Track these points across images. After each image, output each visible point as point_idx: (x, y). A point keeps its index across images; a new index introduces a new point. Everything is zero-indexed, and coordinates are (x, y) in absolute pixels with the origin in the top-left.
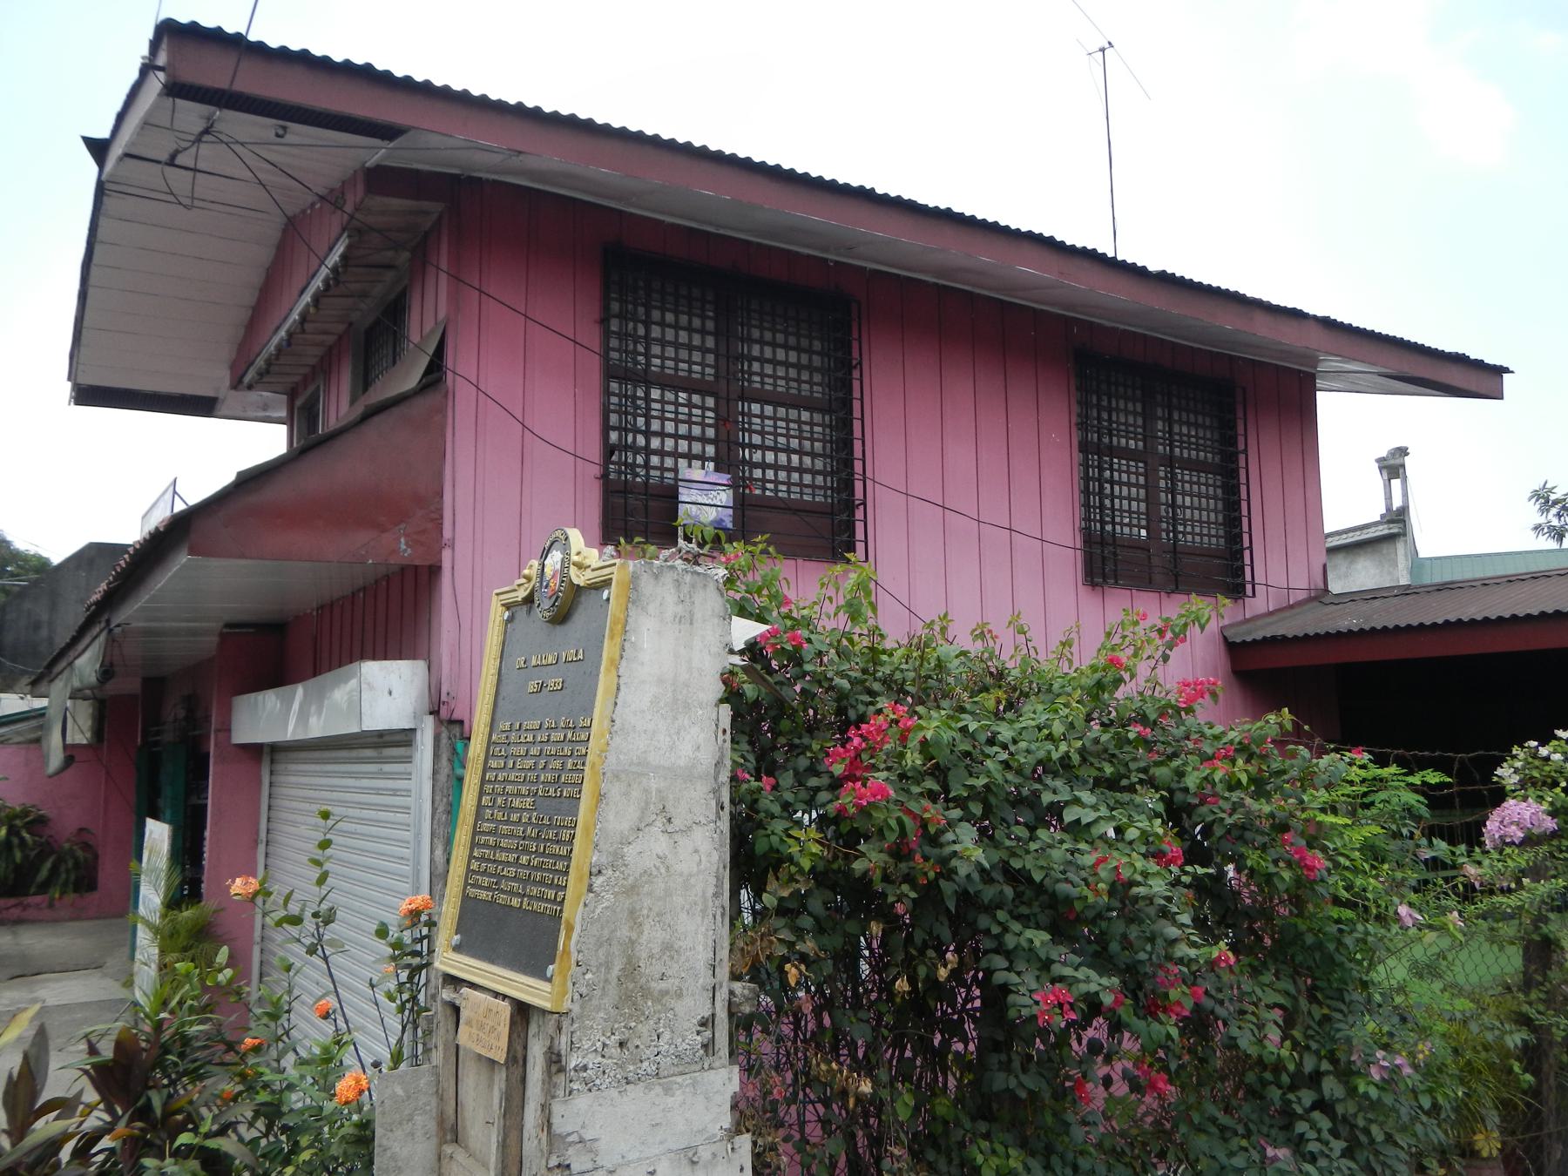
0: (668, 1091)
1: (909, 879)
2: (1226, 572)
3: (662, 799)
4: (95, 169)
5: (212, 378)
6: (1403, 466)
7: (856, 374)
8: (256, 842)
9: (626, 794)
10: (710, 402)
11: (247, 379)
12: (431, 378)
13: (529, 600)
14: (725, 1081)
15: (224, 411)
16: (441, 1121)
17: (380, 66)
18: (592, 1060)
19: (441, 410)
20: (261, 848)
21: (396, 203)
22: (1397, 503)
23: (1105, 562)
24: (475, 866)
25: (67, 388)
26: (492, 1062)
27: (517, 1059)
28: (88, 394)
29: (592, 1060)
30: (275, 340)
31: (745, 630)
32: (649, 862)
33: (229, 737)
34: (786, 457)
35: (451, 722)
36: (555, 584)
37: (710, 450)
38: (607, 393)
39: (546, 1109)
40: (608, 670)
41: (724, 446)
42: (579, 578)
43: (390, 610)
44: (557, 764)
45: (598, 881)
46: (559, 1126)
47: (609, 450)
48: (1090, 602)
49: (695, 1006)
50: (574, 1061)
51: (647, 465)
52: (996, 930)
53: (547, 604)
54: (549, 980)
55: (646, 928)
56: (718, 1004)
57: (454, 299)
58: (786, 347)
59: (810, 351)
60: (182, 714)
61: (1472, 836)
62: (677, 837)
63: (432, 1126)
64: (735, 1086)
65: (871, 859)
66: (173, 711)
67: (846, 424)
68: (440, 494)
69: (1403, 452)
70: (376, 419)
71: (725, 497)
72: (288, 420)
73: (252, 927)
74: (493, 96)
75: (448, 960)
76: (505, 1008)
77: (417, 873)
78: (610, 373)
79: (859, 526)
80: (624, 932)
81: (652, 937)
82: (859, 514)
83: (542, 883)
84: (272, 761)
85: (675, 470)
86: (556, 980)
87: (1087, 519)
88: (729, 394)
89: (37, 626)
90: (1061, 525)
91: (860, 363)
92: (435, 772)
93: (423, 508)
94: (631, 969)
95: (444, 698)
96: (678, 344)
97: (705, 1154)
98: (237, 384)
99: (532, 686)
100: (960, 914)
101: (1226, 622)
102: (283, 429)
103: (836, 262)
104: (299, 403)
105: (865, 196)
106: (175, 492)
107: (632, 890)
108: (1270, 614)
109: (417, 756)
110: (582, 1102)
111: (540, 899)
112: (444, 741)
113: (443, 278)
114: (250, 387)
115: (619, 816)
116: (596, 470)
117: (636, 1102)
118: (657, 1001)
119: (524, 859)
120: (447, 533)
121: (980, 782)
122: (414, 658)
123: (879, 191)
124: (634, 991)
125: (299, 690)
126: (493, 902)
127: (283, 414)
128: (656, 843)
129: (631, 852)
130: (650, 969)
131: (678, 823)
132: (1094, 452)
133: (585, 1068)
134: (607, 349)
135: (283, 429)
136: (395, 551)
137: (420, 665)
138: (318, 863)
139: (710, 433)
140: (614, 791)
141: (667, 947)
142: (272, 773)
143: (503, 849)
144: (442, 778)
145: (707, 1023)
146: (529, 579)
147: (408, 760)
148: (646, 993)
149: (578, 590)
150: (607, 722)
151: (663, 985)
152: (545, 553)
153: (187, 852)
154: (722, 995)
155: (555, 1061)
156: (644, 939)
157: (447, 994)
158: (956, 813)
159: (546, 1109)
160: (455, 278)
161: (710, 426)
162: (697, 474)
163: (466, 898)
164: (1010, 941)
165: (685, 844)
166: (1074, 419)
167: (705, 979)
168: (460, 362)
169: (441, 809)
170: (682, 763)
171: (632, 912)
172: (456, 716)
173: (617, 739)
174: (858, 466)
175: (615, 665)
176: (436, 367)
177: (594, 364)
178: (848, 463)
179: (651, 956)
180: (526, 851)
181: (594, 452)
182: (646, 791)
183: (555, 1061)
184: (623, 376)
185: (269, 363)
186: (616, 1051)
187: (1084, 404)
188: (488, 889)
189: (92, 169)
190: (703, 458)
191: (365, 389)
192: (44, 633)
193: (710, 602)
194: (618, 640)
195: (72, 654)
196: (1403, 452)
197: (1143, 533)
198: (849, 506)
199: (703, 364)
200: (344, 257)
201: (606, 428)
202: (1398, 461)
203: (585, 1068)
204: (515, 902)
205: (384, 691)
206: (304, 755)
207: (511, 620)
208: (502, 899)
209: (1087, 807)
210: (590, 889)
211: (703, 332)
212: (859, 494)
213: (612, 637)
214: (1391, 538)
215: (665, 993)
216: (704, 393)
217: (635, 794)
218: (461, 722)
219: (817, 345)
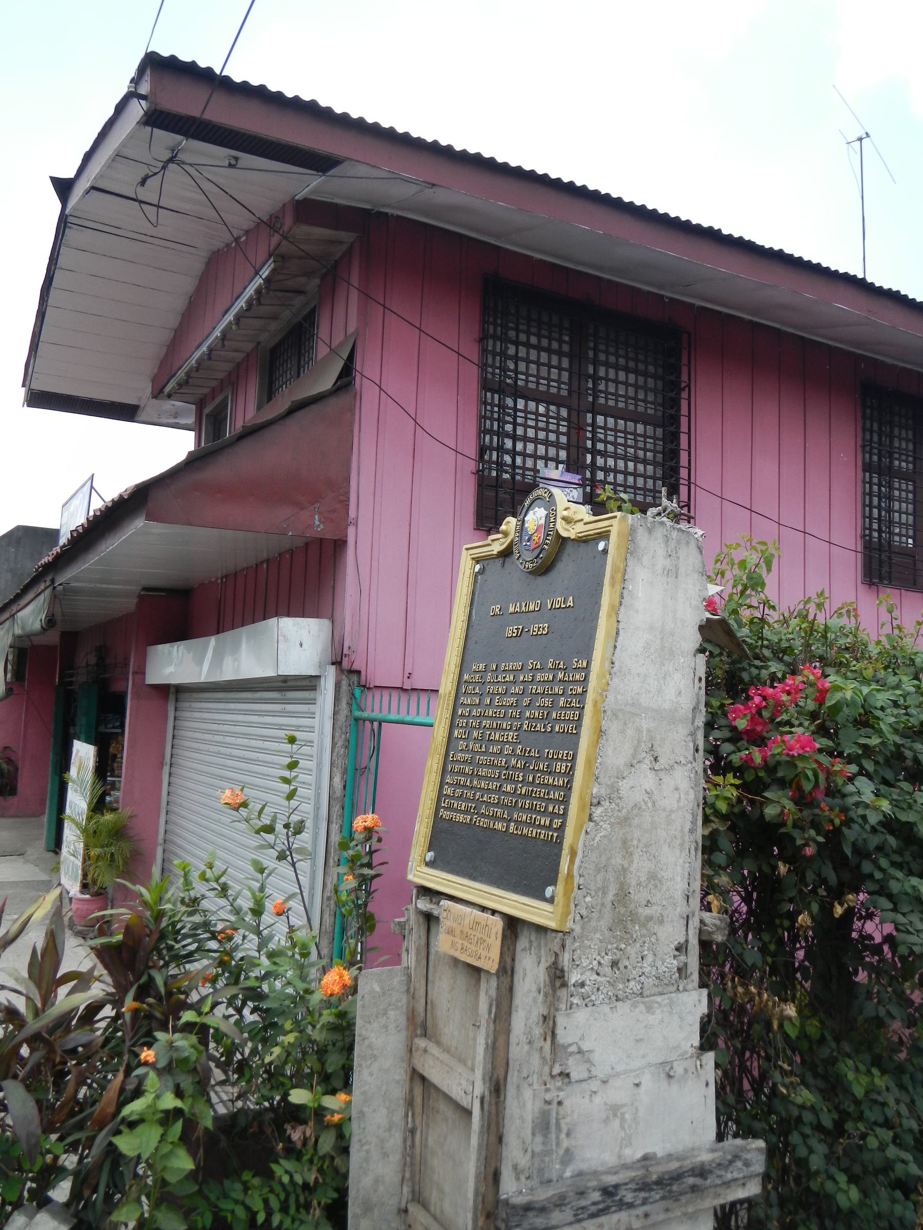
0: (649, 1009)
1: (815, 824)
3: (652, 738)
4: (59, 206)
5: (134, 389)
7: (684, 395)
8: (162, 765)
9: (622, 732)
10: (564, 413)
11: (167, 389)
12: (345, 380)
13: (506, 553)
14: (695, 1003)
15: (143, 415)
16: (411, 1017)
17: (323, 103)
18: (589, 977)
19: (352, 410)
20: (166, 769)
21: (319, 232)
24: (448, 791)
25: (22, 393)
26: (476, 971)
27: (507, 970)
28: (39, 398)
29: (589, 977)
30: (197, 355)
33: (144, 678)
35: (351, 672)
36: (538, 538)
37: (563, 454)
39: (549, 1022)
40: (609, 616)
41: (573, 450)
43: (302, 575)
44: (547, 702)
45: (598, 811)
46: (563, 1037)
47: (482, 450)
49: (672, 932)
50: (574, 977)
52: (878, 875)
53: (528, 556)
54: (551, 901)
55: (636, 857)
56: (691, 932)
57: (363, 314)
58: (627, 370)
59: (645, 374)
60: (93, 660)
62: (662, 775)
63: (403, 1020)
64: (703, 1009)
65: (778, 805)
66: (86, 658)
70: (299, 414)
72: (196, 427)
73: (157, 832)
74: (415, 134)
75: (420, 873)
76: (497, 924)
77: (318, 796)
78: (486, 385)
80: (618, 860)
81: (640, 866)
83: (532, 809)
84: (177, 700)
85: (536, 471)
86: (559, 899)
88: (578, 406)
90: (846, 533)
91: (689, 386)
92: (335, 713)
93: (335, 492)
94: (623, 895)
95: (346, 651)
96: (540, 366)
97: (679, 1069)
98: (158, 393)
99: (510, 631)
102: (192, 434)
103: (671, 299)
104: (207, 411)
105: (712, 236)
106: (92, 487)
107: (625, 821)
109: (320, 701)
110: (581, 1016)
111: (532, 824)
112: (344, 687)
113: (354, 295)
114: (169, 396)
115: (616, 753)
116: (472, 466)
117: (623, 1018)
118: (643, 925)
119: (509, 788)
122: (317, 616)
123: (725, 232)
124: (626, 919)
125: (213, 641)
126: (471, 825)
127: (191, 420)
128: (644, 779)
129: (624, 785)
130: (638, 896)
131: (662, 760)
133: (583, 985)
135: (192, 434)
136: (311, 526)
137: (325, 623)
138: (287, 781)
139: (563, 439)
140: (612, 727)
142: (176, 709)
143: (480, 777)
144: (342, 717)
145: (681, 948)
146: (506, 534)
147: (313, 702)
148: (634, 917)
149: (562, 542)
150: (607, 664)
151: (648, 911)
153: (105, 767)
154: (695, 923)
155: (557, 976)
156: (633, 868)
157: (423, 904)
158: (853, 768)
159: (549, 1022)
160: (365, 295)
161: (563, 434)
163: (437, 818)
164: (894, 886)
165: (669, 782)
166: (860, 443)
167: (681, 908)
169: (340, 744)
170: (667, 706)
171: (625, 842)
172: (355, 667)
173: (616, 681)
174: (683, 473)
175: (616, 609)
176: (347, 371)
177: (472, 374)
179: (639, 884)
180: (509, 779)
181: (472, 452)
182: (639, 730)
183: (557, 976)
184: (496, 387)
185: (188, 374)
186: (608, 970)
188: (466, 812)
189: (55, 205)
190: (558, 462)
191: (269, 399)
194: (618, 587)
195: (14, 608)
203: (583, 985)
204: (499, 826)
205: (294, 643)
206: (202, 695)
207: (482, 572)
208: (483, 822)
210: (590, 819)
211: (560, 354)
213: (613, 585)
215: (650, 918)
216: (559, 406)
217: (630, 732)
218: (358, 673)
219: (651, 369)
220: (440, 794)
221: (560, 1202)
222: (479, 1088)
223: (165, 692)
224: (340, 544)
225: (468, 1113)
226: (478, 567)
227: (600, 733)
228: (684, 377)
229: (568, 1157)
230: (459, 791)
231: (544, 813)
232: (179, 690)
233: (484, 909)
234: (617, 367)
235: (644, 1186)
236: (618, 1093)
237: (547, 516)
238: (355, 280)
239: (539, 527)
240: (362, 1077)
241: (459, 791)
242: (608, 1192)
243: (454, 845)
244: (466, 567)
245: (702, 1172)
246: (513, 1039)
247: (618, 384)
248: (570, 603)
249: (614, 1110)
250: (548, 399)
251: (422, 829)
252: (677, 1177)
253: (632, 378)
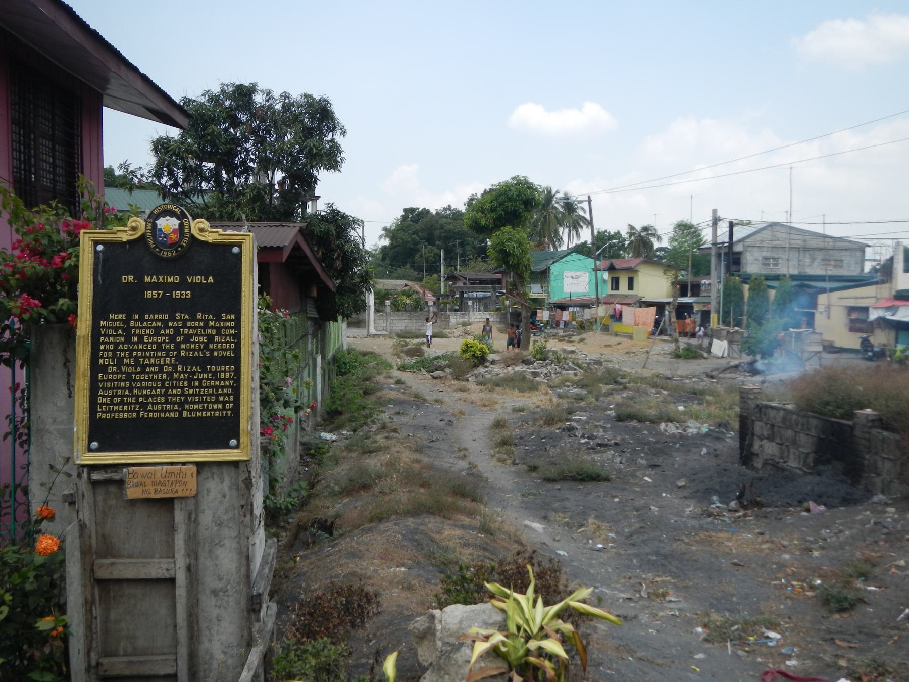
26: (167, 504)
54: (237, 447)
76: (194, 469)
225: (172, 581)
226: (100, 248)
230: (115, 400)
231: (217, 401)
233: (172, 464)
237: (181, 226)
239: (174, 231)
241: (115, 400)
246: (202, 528)
248: (211, 280)
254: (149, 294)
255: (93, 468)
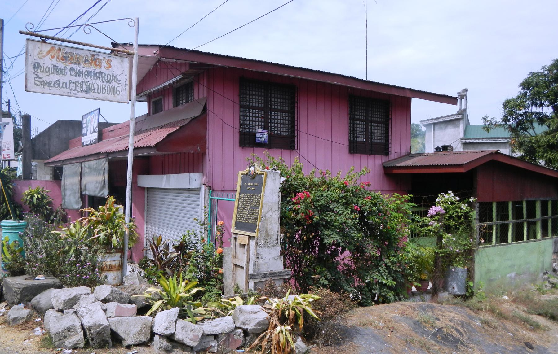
2: (384, 149)
6: (466, 95)
8: (144, 211)
13: (247, 174)
14: (279, 248)
20: (146, 212)
22: (463, 108)
23: (355, 148)
27: (249, 244)
31: (283, 179)
32: (269, 216)
34: (279, 123)
36: (253, 173)
37: (263, 124)
38: (241, 112)
42: (258, 173)
47: (241, 125)
48: (350, 157)
49: (275, 237)
50: (259, 244)
51: (249, 129)
57: (208, 93)
58: (280, 99)
61: (425, 214)
64: (281, 249)
67: (293, 117)
68: (206, 137)
69: (466, 90)
71: (266, 136)
73: (144, 231)
76: (247, 237)
78: (241, 106)
79: (296, 141)
81: (269, 227)
82: (296, 138)
87: (350, 137)
88: (267, 110)
89: (45, 145)
94: (267, 231)
96: (256, 99)
99: (248, 188)
100: (315, 227)
101: (384, 161)
104: (153, 100)
105: (300, 69)
108: (395, 159)
113: (205, 89)
115: (265, 209)
116: (238, 131)
120: (207, 145)
121: (320, 204)
122: (198, 172)
124: (267, 235)
128: (270, 213)
130: (269, 232)
132: (352, 119)
134: (240, 101)
136: (197, 150)
139: (263, 120)
141: (272, 228)
144: (207, 198)
145: (277, 240)
147: (199, 194)
152: (250, 167)
157: (234, 236)
160: (208, 88)
162: (260, 131)
166: (348, 113)
167: (277, 233)
168: (210, 108)
175: (264, 187)
176: (205, 109)
178: (294, 127)
183: (257, 243)
184: (244, 108)
187: (351, 108)
192: (47, 147)
193: (278, 176)
196: (466, 90)
197: (364, 140)
198: (294, 136)
199: (261, 104)
200: (180, 79)
201: (240, 120)
202: (464, 94)
205: (193, 180)
209: (339, 209)
211: (261, 96)
212: (296, 134)
214: (458, 120)
219: (287, 97)
220: (237, 217)
221: (258, 275)
222: (245, 263)
223: (143, 188)
224: (206, 153)
227: (262, 207)
228: (296, 100)
229: (259, 270)
232: (148, 189)
234: (277, 98)
235: (271, 274)
236: (267, 261)
238: (205, 84)
240: (225, 265)
242: (265, 274)
243: (239, 226)
244: (240, 176)
245: (280, 273)
247: (277, 102)
249: (266, 263)
250: (258, 108)
251: (233, 223)
252: (276, 273)
253: (282, 101)
254: (248, 188)
255: (235, 234)
